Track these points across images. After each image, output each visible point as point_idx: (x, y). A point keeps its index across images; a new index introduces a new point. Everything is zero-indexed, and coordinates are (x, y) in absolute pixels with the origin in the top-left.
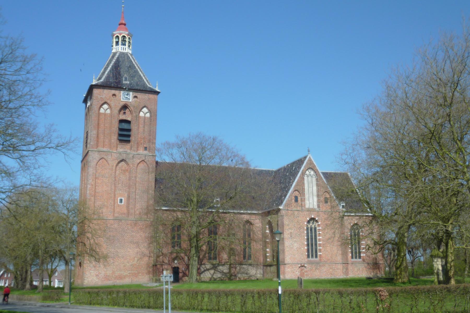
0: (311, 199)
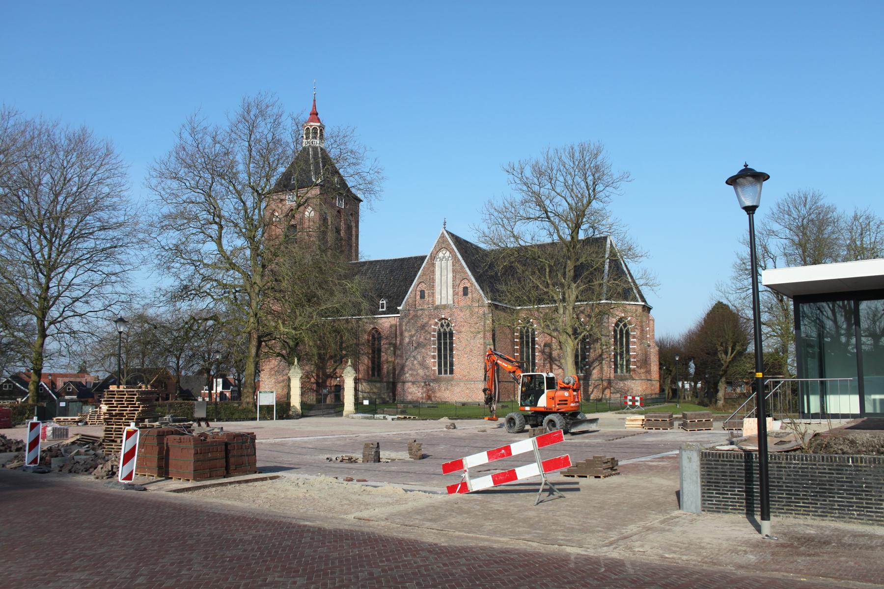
0: (444, 292)
